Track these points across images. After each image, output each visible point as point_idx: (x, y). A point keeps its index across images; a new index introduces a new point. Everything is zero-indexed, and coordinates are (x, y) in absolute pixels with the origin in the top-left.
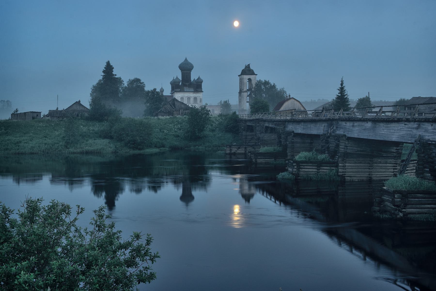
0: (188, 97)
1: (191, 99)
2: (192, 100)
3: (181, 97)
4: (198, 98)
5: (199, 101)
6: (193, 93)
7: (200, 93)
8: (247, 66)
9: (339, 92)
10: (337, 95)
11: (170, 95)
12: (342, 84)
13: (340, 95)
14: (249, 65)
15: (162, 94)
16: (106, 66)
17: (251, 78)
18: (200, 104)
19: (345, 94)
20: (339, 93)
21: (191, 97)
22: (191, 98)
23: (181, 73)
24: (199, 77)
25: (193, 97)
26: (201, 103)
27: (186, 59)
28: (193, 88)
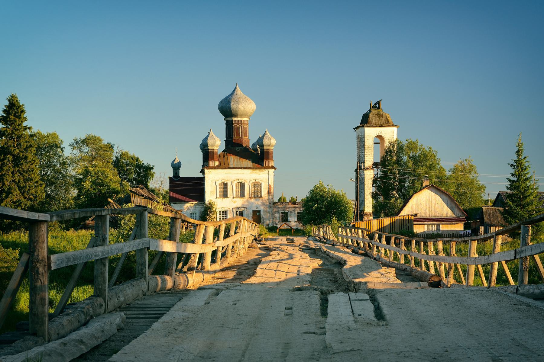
2: (232, 190)
8: (376, 104)
9: (512, 171)
10: (509, 180)
11: (201, 175)
12: (519, 153)
13: (515, 179)
14: (378, 102)
15: (176, 173)
16: (6, 106)
17: (383, 135)
19: (528, 176)
20: (513, 175)
23: (225, 122)
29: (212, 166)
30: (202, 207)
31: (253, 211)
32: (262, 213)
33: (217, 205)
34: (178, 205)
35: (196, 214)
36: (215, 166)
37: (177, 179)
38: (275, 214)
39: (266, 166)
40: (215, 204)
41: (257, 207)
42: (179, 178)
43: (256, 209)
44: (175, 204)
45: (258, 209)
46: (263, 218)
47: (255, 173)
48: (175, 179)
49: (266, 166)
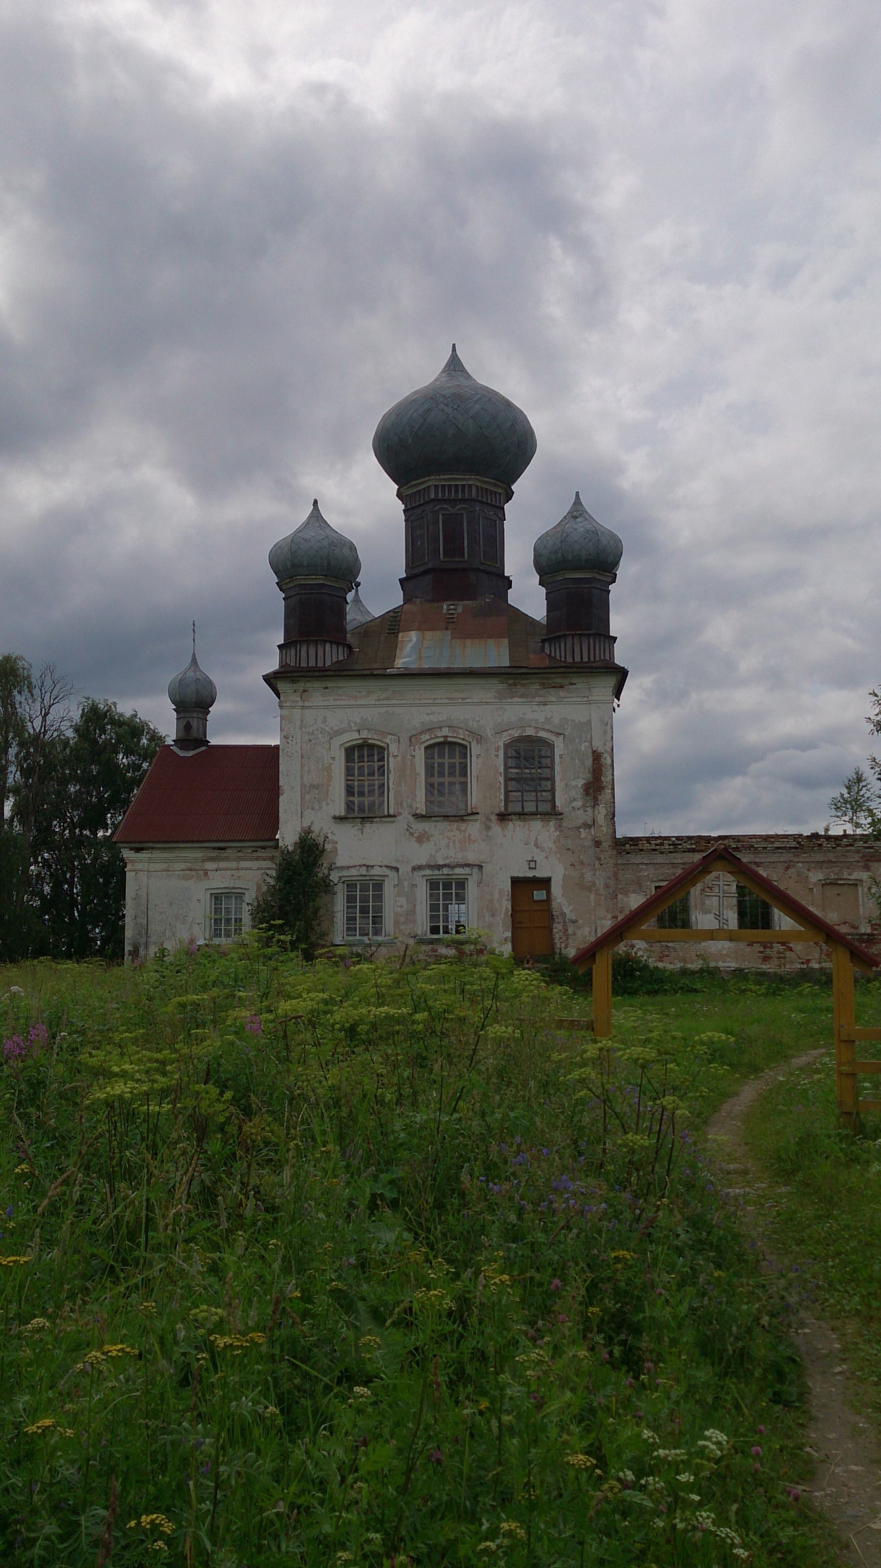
0: (440, 735)
1: (475, 766)
3: (352, 737)
4: (559, 747)
5: (580, 783)
6: (495, 685)
7: (581, 683)
18: (587, 826)
21: (480, 738)
22: (475, 749)
24: (578, 502)
25: (505, 738)
26: (601, 812)
27: (454, 365)
28: (505, 642)
29: (312, 663)
30: (268, 864)
31: (516, 882)
32: (556, 889)
33: (335, 851)
34: (157, 854)
35: (240, 896)
36: (328, 663)
37: (190, 754)
38: (626, 894)
39: (577, 659)
40: (328, 847)
41: (532, 864)
42: (204, 748)
43: (530, 874)
44: (138, 850)
45: (540, 873)
46: (563, 915)
47: (522, 696)
48: (182, 754)
49: (577, 659)
